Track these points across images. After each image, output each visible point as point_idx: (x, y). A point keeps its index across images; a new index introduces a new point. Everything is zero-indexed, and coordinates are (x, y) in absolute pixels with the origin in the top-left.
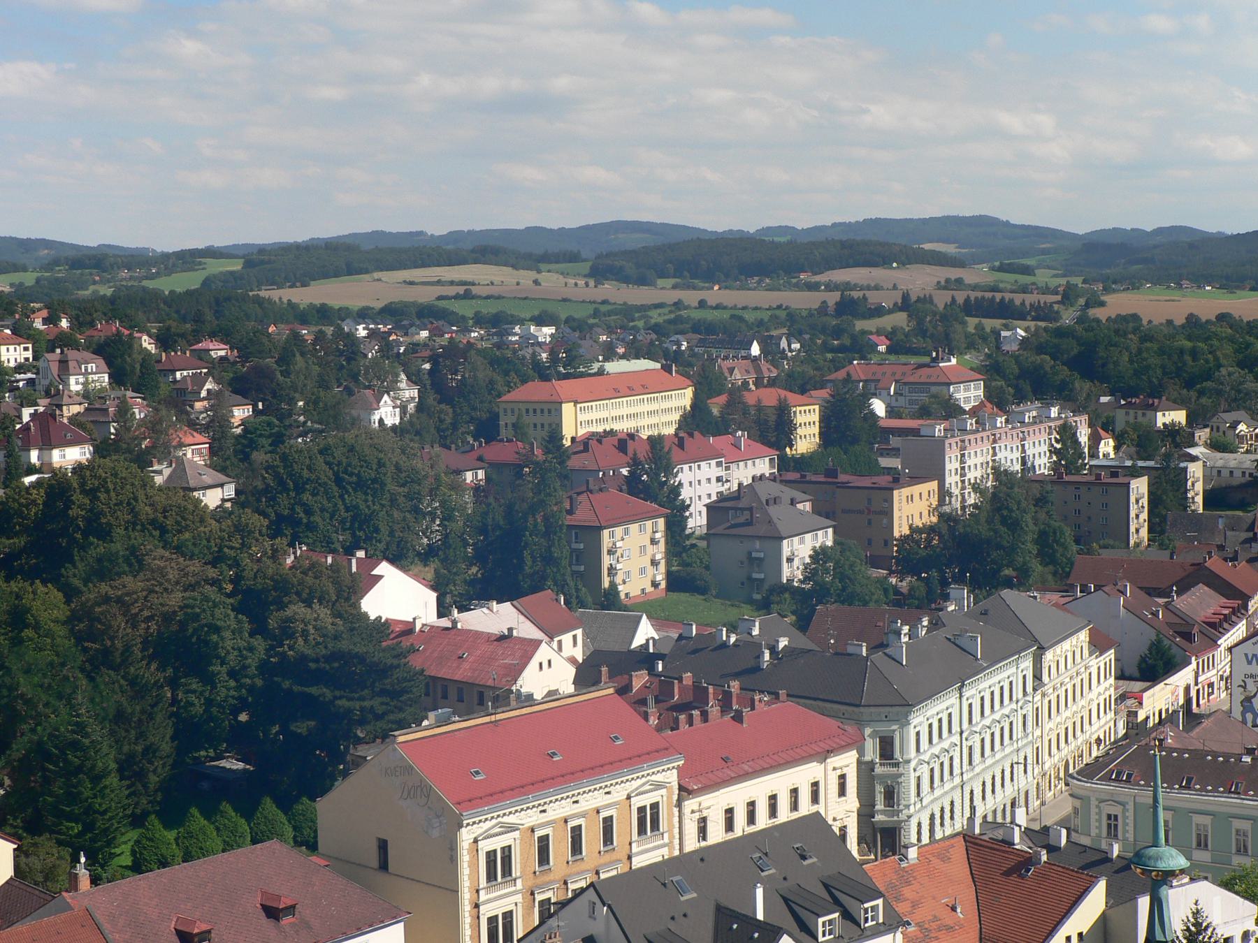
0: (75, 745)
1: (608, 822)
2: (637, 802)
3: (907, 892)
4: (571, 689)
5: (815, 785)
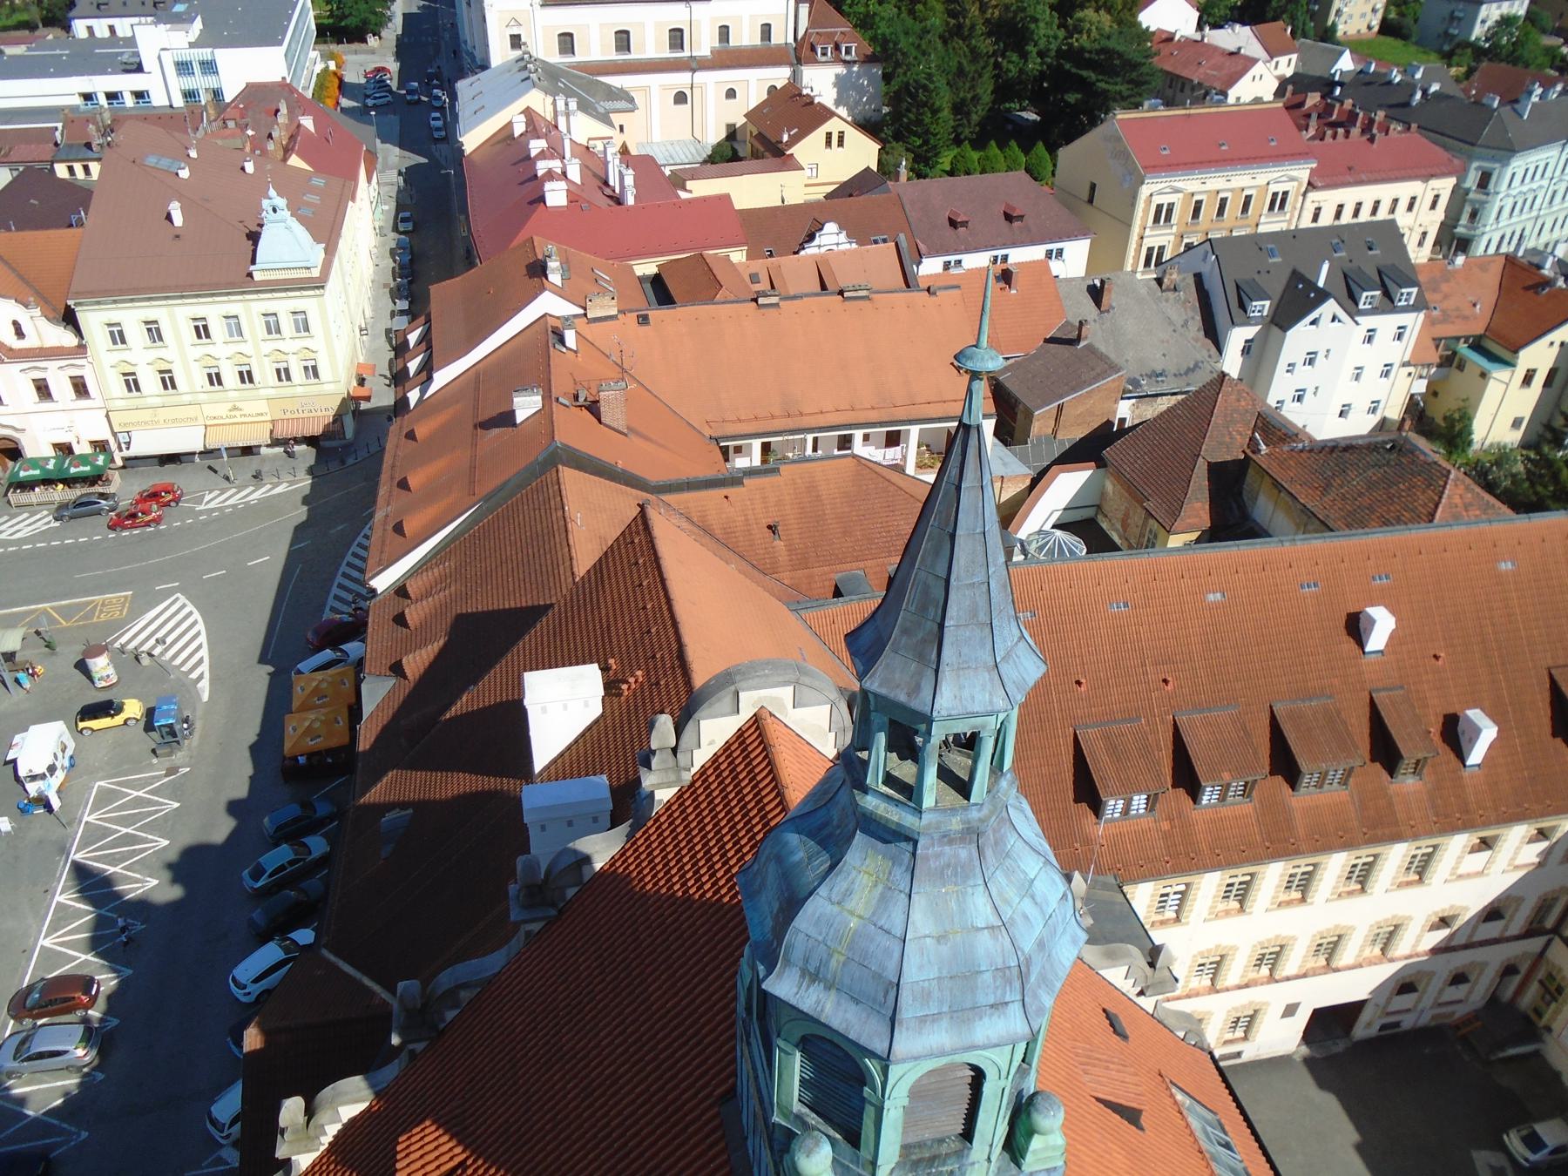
0: (925, 88)
1: (1248, 199)
2: (1273, 188)
3: (1444, 287)
4: (1271, 98)
5: (1414, 199)
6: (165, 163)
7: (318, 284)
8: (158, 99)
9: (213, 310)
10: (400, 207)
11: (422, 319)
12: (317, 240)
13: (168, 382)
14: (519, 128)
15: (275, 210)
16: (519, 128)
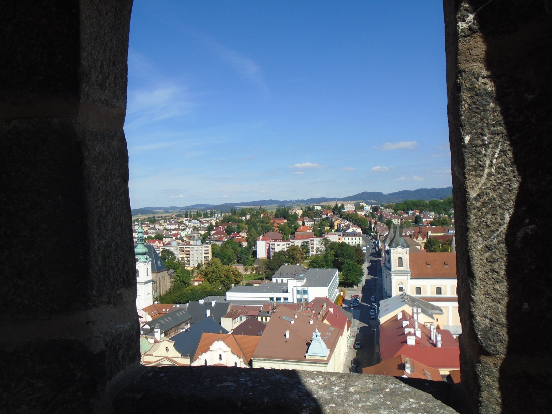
6: (288, 319)
8: (290, 300)
10: (356, 340)
12: (328, 347)
14: (400, 317)
16: (400, 317)
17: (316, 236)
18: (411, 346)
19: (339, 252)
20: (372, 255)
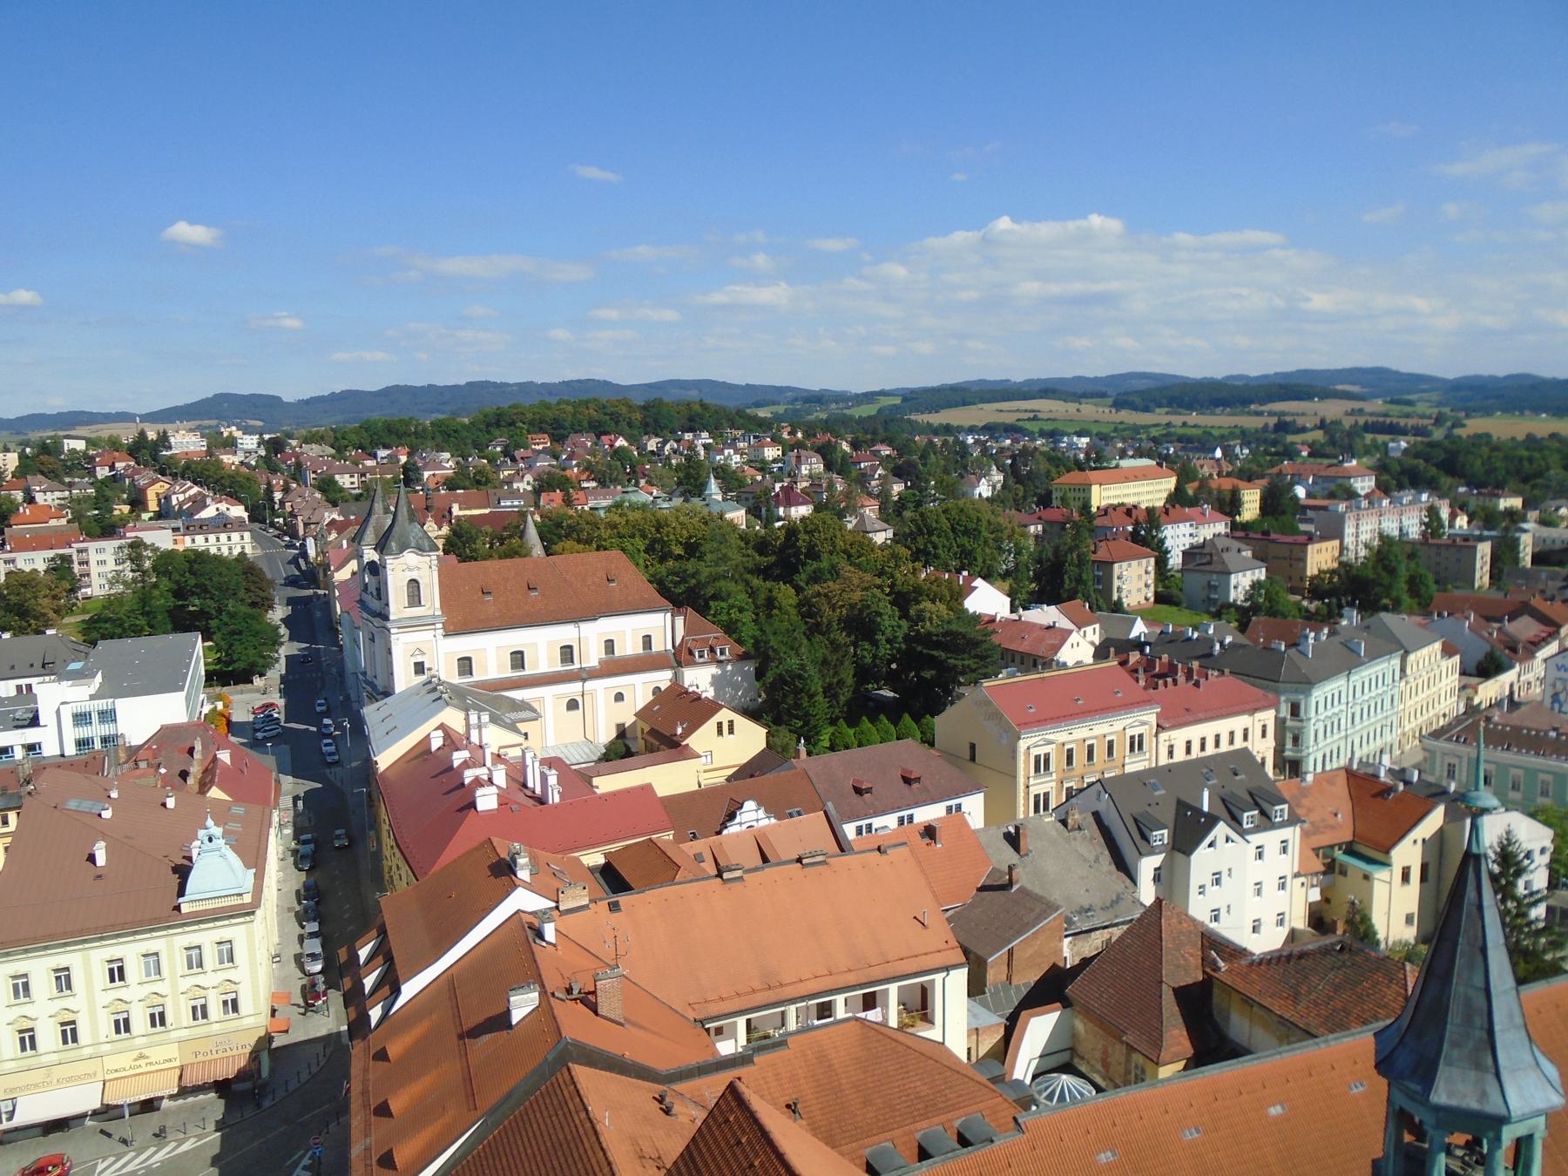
0: (800, 677)
1: (1111, 744)
2: (1130, 732)
3: (1305, 802)
4: (1091, 661)
5: (1246, 730)
7: (247, 911)
8: (50, 749)
9: (130, 951)
11: (374, 933)
12: (248, 866)
13: (69, 1033)
14: (437, 742)
15: (210, 840)
16: (437, 742)
17: (92, 536)
18: (555, 806)
19: (192, 582)
20: (291, 582)
